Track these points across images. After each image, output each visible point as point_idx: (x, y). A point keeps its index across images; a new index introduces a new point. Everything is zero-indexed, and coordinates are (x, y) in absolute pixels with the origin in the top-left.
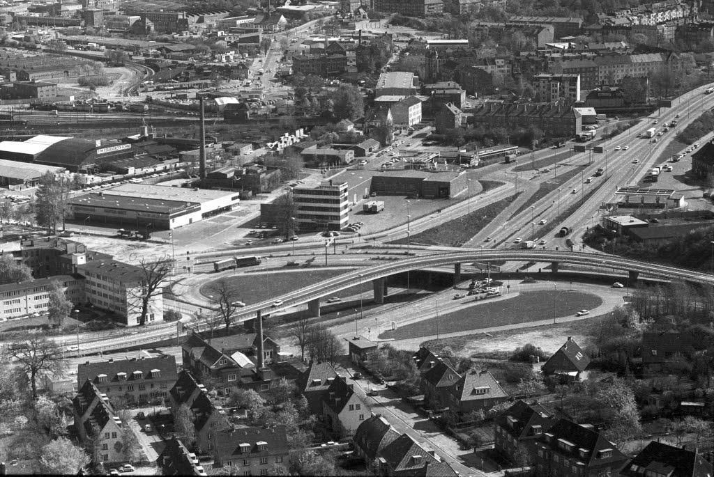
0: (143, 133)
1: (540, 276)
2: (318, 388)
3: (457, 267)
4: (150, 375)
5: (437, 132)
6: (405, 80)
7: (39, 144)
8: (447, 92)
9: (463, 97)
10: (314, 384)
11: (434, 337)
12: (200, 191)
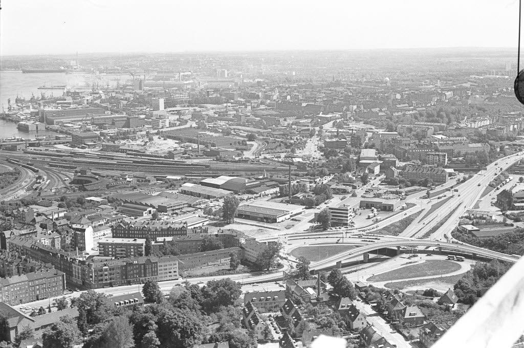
0: (264, 176)
1: (434, 252)
2: (344, 308)
3: (399, 247)
4: (274, 299)
5: (386, 178)
6: (371, 153)
7: (221, 180)
8: (390, 159)
9: (397, 162)
10: (342, 307)
11: (390, 282)
12: (289, 205)
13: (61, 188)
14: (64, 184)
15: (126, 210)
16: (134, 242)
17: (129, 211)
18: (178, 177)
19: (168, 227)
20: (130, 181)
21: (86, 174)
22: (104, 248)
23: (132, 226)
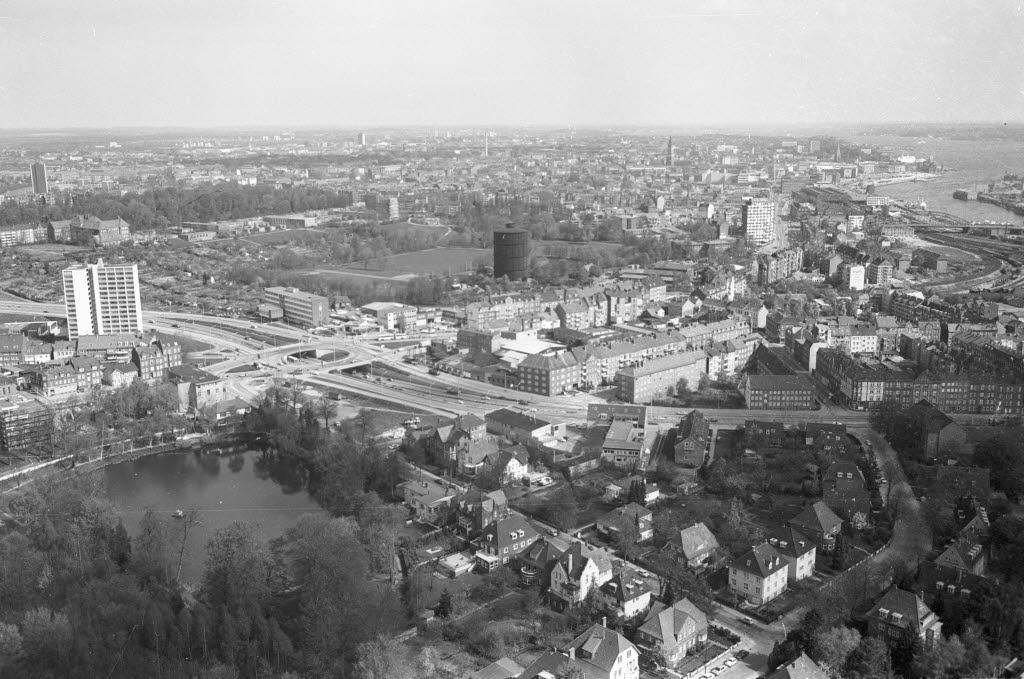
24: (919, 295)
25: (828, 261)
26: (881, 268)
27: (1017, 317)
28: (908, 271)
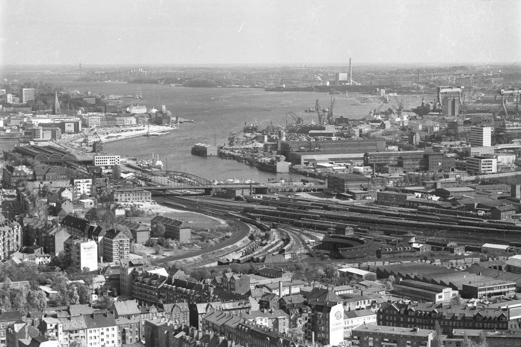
13: (300, 254)
14: (306, 248)
15: (404, 291)
16: (412, 334)
17: (413, 292)
18: (504, 247)
19: (475, 314)
20: (418, 249)
21: (344, 234)
22: (358, 337)
23: (413, 308)
24: (162, 272)
25: (53, 237)
26: (116, 241)
27: (270, 290)
28: (149, 244)
